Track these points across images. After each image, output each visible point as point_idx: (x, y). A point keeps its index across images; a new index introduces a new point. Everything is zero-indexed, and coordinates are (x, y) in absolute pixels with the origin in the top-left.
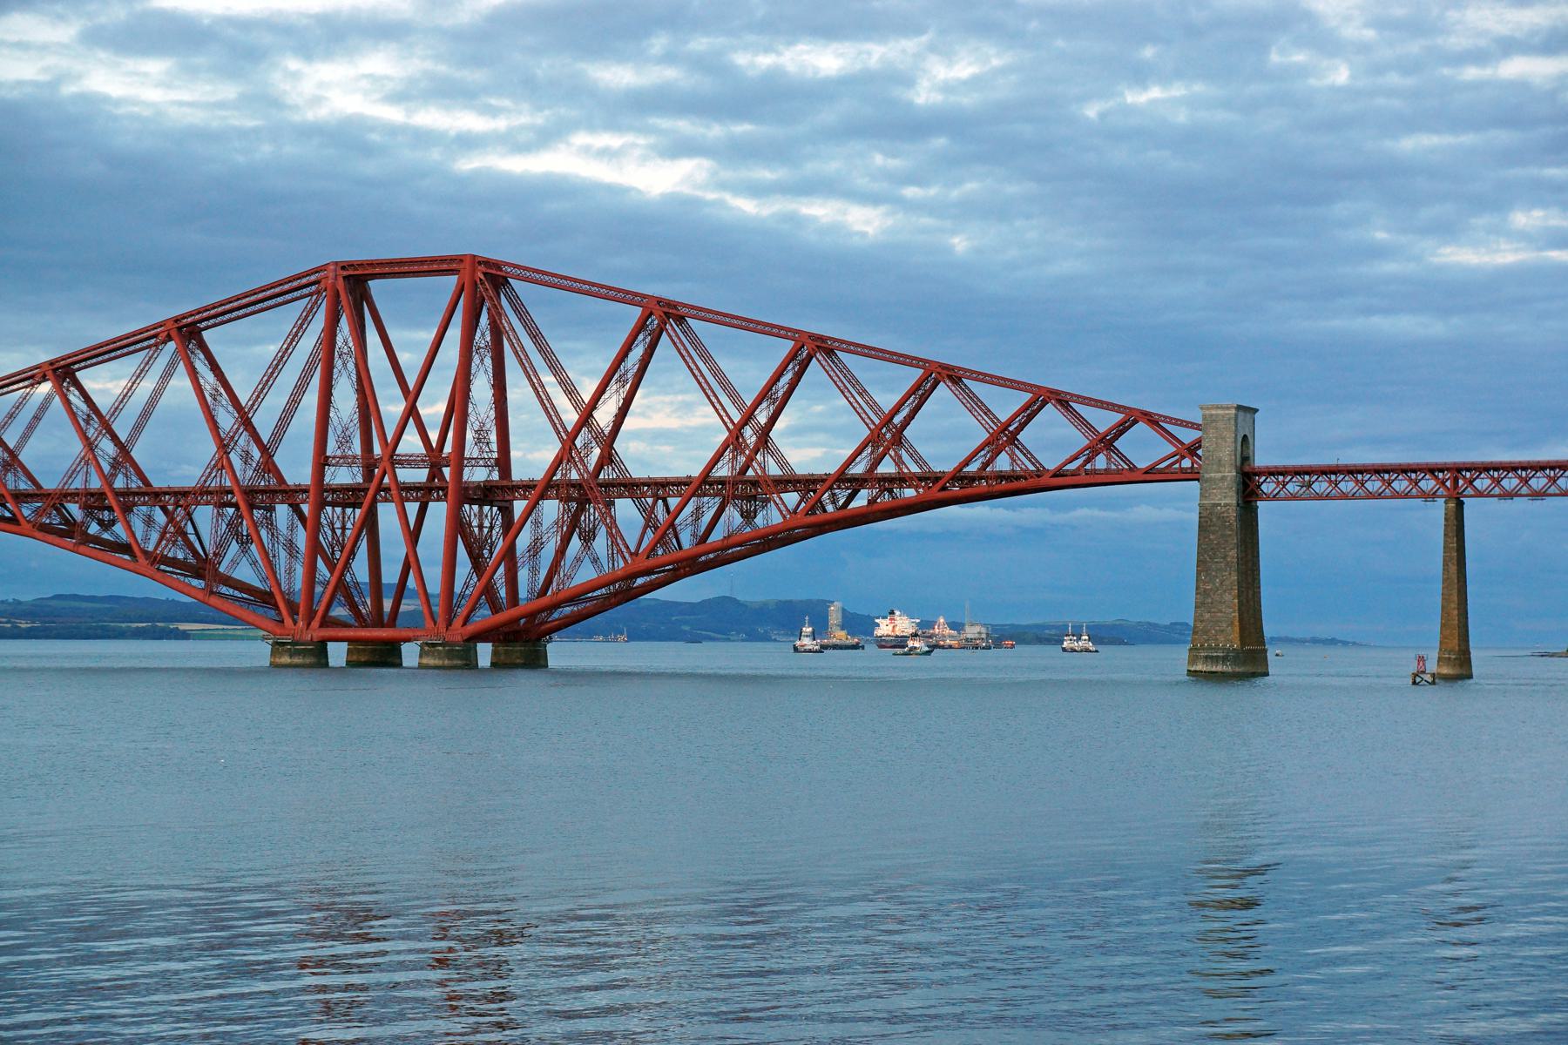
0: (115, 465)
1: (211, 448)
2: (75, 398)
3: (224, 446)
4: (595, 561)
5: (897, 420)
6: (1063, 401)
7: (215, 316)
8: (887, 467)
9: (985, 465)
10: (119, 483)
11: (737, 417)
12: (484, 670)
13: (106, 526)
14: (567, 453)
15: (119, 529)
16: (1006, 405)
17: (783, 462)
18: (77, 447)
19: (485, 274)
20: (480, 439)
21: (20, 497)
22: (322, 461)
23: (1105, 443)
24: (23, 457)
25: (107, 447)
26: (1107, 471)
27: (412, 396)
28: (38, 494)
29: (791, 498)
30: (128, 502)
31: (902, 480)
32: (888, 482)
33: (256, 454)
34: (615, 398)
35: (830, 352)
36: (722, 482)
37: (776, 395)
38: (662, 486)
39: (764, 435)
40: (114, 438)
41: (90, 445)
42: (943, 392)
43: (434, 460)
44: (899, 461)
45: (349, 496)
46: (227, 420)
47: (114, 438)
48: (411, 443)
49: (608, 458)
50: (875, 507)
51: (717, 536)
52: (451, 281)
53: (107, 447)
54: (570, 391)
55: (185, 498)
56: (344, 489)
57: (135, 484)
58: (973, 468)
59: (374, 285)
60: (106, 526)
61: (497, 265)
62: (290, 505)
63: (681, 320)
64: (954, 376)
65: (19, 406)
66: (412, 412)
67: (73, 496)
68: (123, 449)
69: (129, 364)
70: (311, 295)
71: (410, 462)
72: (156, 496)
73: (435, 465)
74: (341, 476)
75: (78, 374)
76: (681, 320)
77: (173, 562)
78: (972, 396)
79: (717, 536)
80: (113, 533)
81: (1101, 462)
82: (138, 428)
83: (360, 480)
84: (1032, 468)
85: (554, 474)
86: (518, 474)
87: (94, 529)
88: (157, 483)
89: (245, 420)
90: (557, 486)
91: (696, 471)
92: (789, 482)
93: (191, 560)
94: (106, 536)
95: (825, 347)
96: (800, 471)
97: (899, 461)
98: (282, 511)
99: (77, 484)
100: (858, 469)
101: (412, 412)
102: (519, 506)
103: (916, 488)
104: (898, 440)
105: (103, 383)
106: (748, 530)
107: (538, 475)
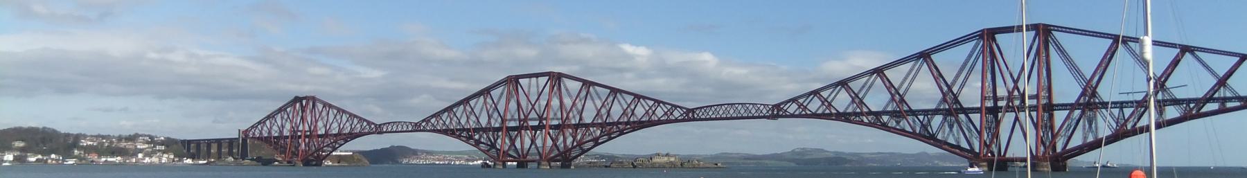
1: (942, 95)
8: (1222, 93)
13: (898, 123)
14: (1083, 94)
24: (864, 101)
28: (870, 113)
31: (1230, 99)
32: (1224, 100)
38: (1121, 105)
39: (633, 111)
41: (893, 96)
46: (945, 89)
48: (1016, 93)
49: (1094, 94)
55: (925, 112)
56: (987, 108)
57: (906, 108)
59: (998, 37)
60: (898, 123)
65: (866, 83)
67: (885, 112)
69: (906, 67)
71: (1017, 99)
72: (914, 113)
73: (541, 118)
74: (989, 104)
75: (885, 72)
80: (900, 126)
82: (907, 90)
83: (993, 105)
86: (1056, 100)
87: (893, 123)
90: (1080, 105)
92: (1176, 102)
94: (898, 127)
95: (1185, 49)
99: (889, 109)
103: (1240, 102)
105: (895, 75)
107: (1073, 100)
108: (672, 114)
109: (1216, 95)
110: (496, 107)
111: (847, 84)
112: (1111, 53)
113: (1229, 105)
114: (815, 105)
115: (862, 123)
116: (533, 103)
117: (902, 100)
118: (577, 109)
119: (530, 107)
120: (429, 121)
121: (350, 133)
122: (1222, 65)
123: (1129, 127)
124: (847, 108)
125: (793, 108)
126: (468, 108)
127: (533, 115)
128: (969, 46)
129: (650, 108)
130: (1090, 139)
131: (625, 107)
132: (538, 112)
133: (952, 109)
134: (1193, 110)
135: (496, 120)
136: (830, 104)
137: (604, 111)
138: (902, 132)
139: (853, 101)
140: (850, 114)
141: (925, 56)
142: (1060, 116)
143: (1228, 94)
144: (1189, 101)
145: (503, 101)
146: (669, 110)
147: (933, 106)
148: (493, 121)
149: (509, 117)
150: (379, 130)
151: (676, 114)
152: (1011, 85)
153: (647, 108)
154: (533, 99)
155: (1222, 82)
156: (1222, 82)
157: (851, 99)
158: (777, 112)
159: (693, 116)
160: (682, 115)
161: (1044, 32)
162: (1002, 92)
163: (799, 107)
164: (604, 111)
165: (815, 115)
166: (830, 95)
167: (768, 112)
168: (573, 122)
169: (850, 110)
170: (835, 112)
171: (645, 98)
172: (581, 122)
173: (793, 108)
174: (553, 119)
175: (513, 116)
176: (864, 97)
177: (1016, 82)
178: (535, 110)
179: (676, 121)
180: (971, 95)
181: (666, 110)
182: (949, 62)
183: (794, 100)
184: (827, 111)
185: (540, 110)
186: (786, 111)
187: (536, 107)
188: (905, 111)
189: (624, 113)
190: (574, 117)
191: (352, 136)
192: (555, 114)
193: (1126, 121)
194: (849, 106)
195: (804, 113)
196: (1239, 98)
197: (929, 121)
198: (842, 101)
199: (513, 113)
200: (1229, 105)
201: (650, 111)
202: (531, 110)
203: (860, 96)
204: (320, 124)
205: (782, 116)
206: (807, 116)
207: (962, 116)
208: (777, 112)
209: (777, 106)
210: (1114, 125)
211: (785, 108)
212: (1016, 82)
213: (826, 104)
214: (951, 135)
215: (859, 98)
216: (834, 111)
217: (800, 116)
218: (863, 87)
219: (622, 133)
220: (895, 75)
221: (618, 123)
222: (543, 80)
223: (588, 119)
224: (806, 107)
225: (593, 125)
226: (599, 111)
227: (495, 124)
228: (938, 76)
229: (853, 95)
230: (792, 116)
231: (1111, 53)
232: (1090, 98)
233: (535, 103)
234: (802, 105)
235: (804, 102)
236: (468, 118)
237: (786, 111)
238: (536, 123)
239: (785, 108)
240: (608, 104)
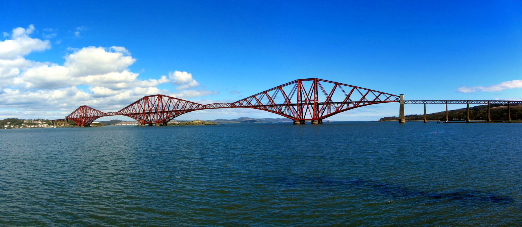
1: (285, 100)
3: (286, 100)
13: (272, 109)
14: (327, 100)
25: (271, 101)
28: (263, 106)
31: (366, 102)
32: (364, 102)
38: (338, 103)
40: (272, 100)
42: (370, 91)
46: (286, 98)
47: (272, 100)
48: (308, 99)
49: (330, 100)
52: (313, 81)
53: (271, 101)
55: (280, 105)
56: (299, 104)
60: (272, 109)
61: (317, 79)
72: (277, 105)
74: (300, 102)
76: (339, 85)
78: (372, 93)
87: (270, 109)
88: (276, 104)
90: (326, 103)
91: (343, 101)
92: (352, 102)
94: (271, 110)
95: (355, 87)
96: (353, 101)
99: (269, 104)
102: (303, 106)
105: (270, 94)
107: (324, 102)
108: (198, 107)
109: (362, 101)
110: (141, 106)
111: (255, 97)
112: (335, 87)
113: (365, 103)
114: (245, 103)
115: (260, 109)
117: (273, 102)
118: (167, 106)
119: (152, 106)
120: (120, 112)
121: (97, 116)
122: (364, 92)
123: (340, 110)
124: (255, 104)
125: (238, 104)
126: (133, 107)
127: (153, 109)
129: (191, 105)
130: (329, 113)
131: (183, 105)
132: (155, 107)
133: (288, 104)
134: (357, 105)
136: (250, 103)
137: (176, 107)
138: (273, 112)
139: (257, 102)
140: (256, 106)
141: (280, 87)
142: (320, 106)
143: (365, 101)
144: (355, 102)
145: (144, 104)
146: (197, 106)
147: (282, 103)
148: (140, 111)
149: (145, 109)
150: (106, 115)
151: (200, 107)
152: (306, 97)
153: (190, 105)
154: (153, 103)
155: (364, 97)
156: (364, 97)
158: (233, 106)
159: (205, 107)
160: (202, 107)
161: (316, 81)
162: (303, 99)
163: (240, 104)
164: (176, 107)
165: (245, 107)
166: (250, 100)
167: (230, 106)
168: (166, 110)
169: (256, 105)
171: (189, 102)
173: (238, 104)
175: (147, 109)
176: (261, 100)
177: (308, 96)
179: (200, 109)
180: (294, 101)
181: (196, 106)
182: (287, 90)
183: (238, 102)
184: (249, 105)
187: (154, 106)
188: (274, 105)
189: (183, 107)
191: (98, 117)
193: (339, 108)
194: (256, 103)
195: (241, 106)
196: (368, 102)
197: (281, 108)
198: (254, 102)
199: (147, 108)
200: (366, 103)
203: (260, 100)
205: (234, 107)
206: (242, 107)
207: (291, 107)
208: (233, 106)
209: (233, 104)
210: (336, 109)
211: (235, 104)
212: (308, 96)
213: (249, 103)
216: (251, 105)
217: (240, 107)
218: (260, 97)
219: (182, 113)
220: (270, 94)
221: (181, 110)
222: (156, 97)
223: (171, 109)
224: (242, 104)
225: (173, 111)
226: (174, 107)
228: (284, 93)
229: (257, 100)
230: (238, 107)
231: (335, 88)
232: (329, 101)
234: (241, 103)
236: (133, 110)
238: (154, 111)
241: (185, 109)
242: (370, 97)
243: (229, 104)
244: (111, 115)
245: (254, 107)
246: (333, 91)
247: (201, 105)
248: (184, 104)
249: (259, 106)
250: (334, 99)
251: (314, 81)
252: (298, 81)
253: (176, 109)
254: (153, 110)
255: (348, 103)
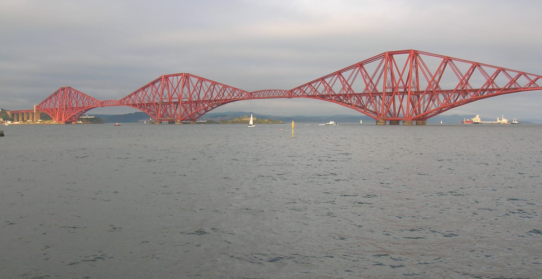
0: (315, 92)
1: (365, 86)
2: (341, 78)
3: (367, 85)
4: (435, 105)
5: (492, 78)
6: (525, 74)
7: (365, 62)
8: (490, 87)
9: (509, 87)
10: (349, 93)
11: (462, 78)
12: (388, 125)
14: (430, 85)
15: (349, 100)
16: (514, 75)
17: (470, 87)
18: (342, 86)
19: (414, 53)
20: (414, 83)
21: (332, 95)
22: (385, 88)
23: (533, 82)
26: (534, 87)
27: (401, 76)
29: (472, 93)
30: (351, 95)
31: (493, 90)
33: (373, 87)
34: (438, 75)
35: (479, 66)
36: (459, 90)
37: (469, 74)
38: (447, 91)
40: (348, 85)
41: (344, 86)
43: (405, 87)
44: (493, 86)
45: (390, 94)
46: (368, 81)
47: (348, 85)
48: (401, 84)
49: (437, 86)
50: (488, 95)
51: (458, 100)
54: (430, 74)
55: (361, 95)
57: (352, 93)
58: (507, 87)
59: (395, 56)
60: (347, 100)
61: (417, 51)
62: (379, 96)
63: (451, 60)
64: (503, 70)
66: (401, 79)
67: (341, 95)
68: (350, 87)
70: (382, 58)
71: (401, 88)
72: (355, 95)
74: (389, 90)
76: (451, 60)
77: (359, 107)
78: (507, 73)
79: (458, 100)
80: (348, 101)
81: (532, 86)
83: (392, 91)
84: (519, 87)
85: (428, 89)
87: (345, 101)
88: (356, 92)
89: (371, 81)
93: (362, 106)
94: (347, 102)
95: (479, 65)
96: (474, 88)
97: (493, 86)
98: (378, 97)
99: (342, 93)
100: (485, 88)
101: (401, 79)
102: (421, 96)
104: (493, 82)
106: (464, 99)
108: (241, 95)
114: (308, 91)
115: (331, 100)
116: (175, 89)
117: (350, 88)
119: (173, 91)
124: (323, 92)
127: (175, 96)
128: (379, 61)
129: (231, 92)
131: (219, 91)
135: (158, 99)
136: (316, 90)
137: (209, 94)
139: (326, 87)
140: (323, 95)
141: (361, 65)
147: (361, 92)
148: (155, 99)
153: (229, 93)
157: (324, 87)
158: (290, 94)
161: (414, 55)
165: (308, 96)
167: (286, 94)
168: (194, 100)
169: (324, 94)
170: (319, 94)
172: (199, 100)
174: (184, 98)
178: (176, 93)
179: (243, 99)
182: (370, 68)
183: (299, 88)
185: (179, 93)
186: (295, 94)
187: (177, 90)
188: (350, 95)
189: (218, 95)
190: (195, 97)
192: (186, 96)
196: (499, 89)
198: (321, 89)
199: (165, 95)
201: (231, 94)
202: (174, 92)
203: (330, 85)
204: (74, 102)
205: (294, 97)
208: (290, 94)
209: (292, 91)
214: (371, 106)
215: (329, 86)
218: (330, 81)
221: (215, 101)
224: (304, 92)
225: (203, 101)
226: (206, 94)
227: (157, 101)
229: (326, 85)
230: (298, 96)
233: (176, 88)
235: (303, 89)
236: (144, 98)
237: (295, 94)
239: (295, 92)
240: (211, 90)
241: (222, 98)
242: (502, 81)
243: (285, 91)
244: (110, 106)
245: (323, 97)
246: (441, 72)
247: (245, 91)
248: (221, 88)
249: (328, 95)
250: (444, 85)
251: (410, 55)
252: (386, 55)
253: (210, 97)
254: (174, 98)
255: (465, 92)
